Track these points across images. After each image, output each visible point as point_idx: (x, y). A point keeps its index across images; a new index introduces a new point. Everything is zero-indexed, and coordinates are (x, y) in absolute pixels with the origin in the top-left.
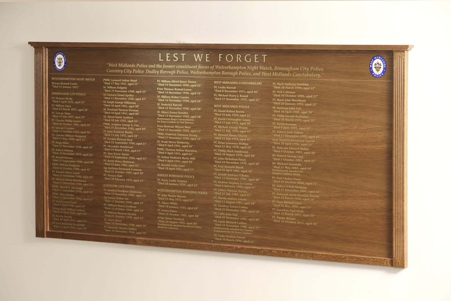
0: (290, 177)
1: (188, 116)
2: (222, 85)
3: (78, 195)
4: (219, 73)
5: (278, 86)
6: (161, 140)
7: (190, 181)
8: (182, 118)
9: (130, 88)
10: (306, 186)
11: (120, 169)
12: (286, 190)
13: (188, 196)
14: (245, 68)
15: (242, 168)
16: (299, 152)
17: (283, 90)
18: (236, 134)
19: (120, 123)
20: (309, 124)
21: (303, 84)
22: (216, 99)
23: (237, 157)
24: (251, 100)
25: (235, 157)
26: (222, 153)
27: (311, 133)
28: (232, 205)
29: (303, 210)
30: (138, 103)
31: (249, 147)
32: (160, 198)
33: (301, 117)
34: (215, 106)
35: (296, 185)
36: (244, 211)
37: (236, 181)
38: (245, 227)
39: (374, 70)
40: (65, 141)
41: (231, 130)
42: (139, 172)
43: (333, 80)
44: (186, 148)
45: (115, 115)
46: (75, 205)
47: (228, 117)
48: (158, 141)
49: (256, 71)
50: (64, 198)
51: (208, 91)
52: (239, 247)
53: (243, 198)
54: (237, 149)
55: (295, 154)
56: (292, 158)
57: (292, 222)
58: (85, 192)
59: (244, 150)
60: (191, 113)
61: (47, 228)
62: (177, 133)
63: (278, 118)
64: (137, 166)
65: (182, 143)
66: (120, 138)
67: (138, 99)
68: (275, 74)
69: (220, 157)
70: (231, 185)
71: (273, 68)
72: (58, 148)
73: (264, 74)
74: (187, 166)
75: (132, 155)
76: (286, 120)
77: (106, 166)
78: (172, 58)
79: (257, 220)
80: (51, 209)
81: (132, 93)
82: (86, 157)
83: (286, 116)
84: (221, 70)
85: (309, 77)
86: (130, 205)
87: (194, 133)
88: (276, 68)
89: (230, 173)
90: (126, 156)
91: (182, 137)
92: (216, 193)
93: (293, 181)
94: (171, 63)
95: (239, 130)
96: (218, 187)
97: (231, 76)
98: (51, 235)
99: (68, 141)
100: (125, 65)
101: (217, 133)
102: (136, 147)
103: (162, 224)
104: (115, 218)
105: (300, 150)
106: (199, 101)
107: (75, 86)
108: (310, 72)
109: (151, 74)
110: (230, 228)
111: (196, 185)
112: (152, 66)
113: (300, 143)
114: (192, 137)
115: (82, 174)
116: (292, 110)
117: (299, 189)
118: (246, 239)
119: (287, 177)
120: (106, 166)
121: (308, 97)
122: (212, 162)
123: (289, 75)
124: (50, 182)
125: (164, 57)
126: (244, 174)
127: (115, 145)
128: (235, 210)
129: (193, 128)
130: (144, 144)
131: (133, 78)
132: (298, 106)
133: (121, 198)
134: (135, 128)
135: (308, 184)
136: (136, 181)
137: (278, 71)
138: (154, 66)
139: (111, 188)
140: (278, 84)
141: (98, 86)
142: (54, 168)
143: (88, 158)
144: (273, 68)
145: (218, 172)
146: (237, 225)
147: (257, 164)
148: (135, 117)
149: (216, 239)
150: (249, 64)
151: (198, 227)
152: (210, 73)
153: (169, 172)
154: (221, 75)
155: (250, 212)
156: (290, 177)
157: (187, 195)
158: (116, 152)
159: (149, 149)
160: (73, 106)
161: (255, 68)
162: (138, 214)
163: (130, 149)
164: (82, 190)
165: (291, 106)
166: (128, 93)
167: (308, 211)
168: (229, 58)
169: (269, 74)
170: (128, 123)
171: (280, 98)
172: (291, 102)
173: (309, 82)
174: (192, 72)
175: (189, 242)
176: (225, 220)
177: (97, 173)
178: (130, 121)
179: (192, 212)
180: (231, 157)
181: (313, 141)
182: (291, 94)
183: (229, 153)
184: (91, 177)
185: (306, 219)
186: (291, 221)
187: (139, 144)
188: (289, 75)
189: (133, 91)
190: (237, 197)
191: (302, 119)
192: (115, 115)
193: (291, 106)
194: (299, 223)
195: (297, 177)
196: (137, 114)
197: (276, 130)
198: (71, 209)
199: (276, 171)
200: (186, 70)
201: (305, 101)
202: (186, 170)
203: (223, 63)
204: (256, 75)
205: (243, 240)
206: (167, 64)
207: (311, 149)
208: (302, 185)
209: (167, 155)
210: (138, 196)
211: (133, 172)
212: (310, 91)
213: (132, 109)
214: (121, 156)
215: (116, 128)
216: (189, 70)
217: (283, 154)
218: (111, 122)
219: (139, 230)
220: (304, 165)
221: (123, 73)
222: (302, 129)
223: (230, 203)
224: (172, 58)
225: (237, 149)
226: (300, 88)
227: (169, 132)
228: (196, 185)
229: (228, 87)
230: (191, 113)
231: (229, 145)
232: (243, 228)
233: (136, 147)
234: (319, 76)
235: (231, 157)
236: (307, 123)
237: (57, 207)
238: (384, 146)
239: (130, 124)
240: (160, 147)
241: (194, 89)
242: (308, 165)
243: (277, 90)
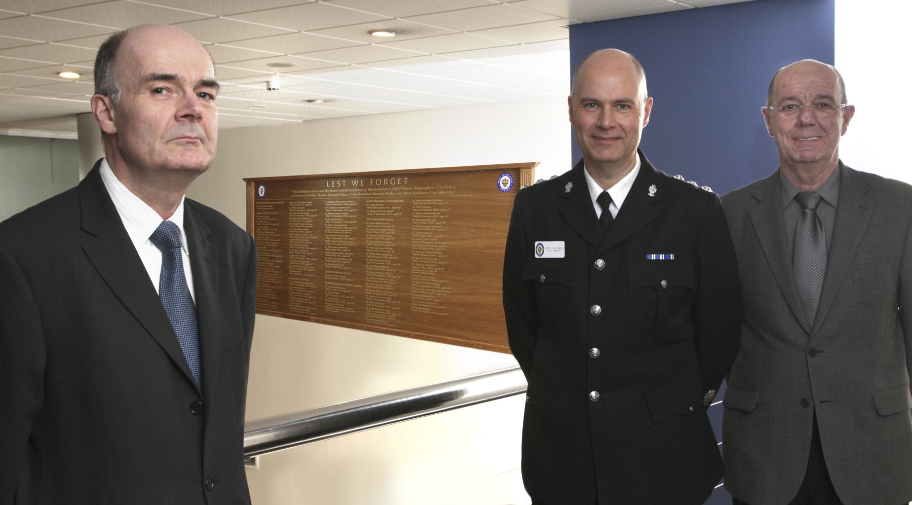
3: (272, 284)
7: (348, 277)
9: (307, 208)
13: (347, 288)
27: (444, 240)
30: (312, 218)
39: (502, 185)
42: (313, 269)
43: (464, 196)
51: (362, 209)
60: (349, 225)
74: (346, 265)
75: (308, 256)
84: (372, 192)
94: (336, 188)
100: (304, 191)
102: (311, 251)
103: (328, 308)
107: (271, 208)
108: (444, 190)
122: (365, 262)
123: (426, 193)
125: (330, 184)
129: (351, 236)
141: (286, 207)
153: (333, 270)
159: (319, 253)
160: (270, 222)
162: (312, 300)
167: (440, 304)
168: (379, 182)
179: (349, 300)
185: (439, 310)
186: (426, 311)
188: (426, 193)
199: (414, 270)
203: (374, 186)
204: (399, 194)
206: (333, 189)
207: (444, 253)
216: (348, 193)
219: (312, 311)
230: (349, 225)
233: (311, 251)
241: (352, 207)
242: (441, 266)
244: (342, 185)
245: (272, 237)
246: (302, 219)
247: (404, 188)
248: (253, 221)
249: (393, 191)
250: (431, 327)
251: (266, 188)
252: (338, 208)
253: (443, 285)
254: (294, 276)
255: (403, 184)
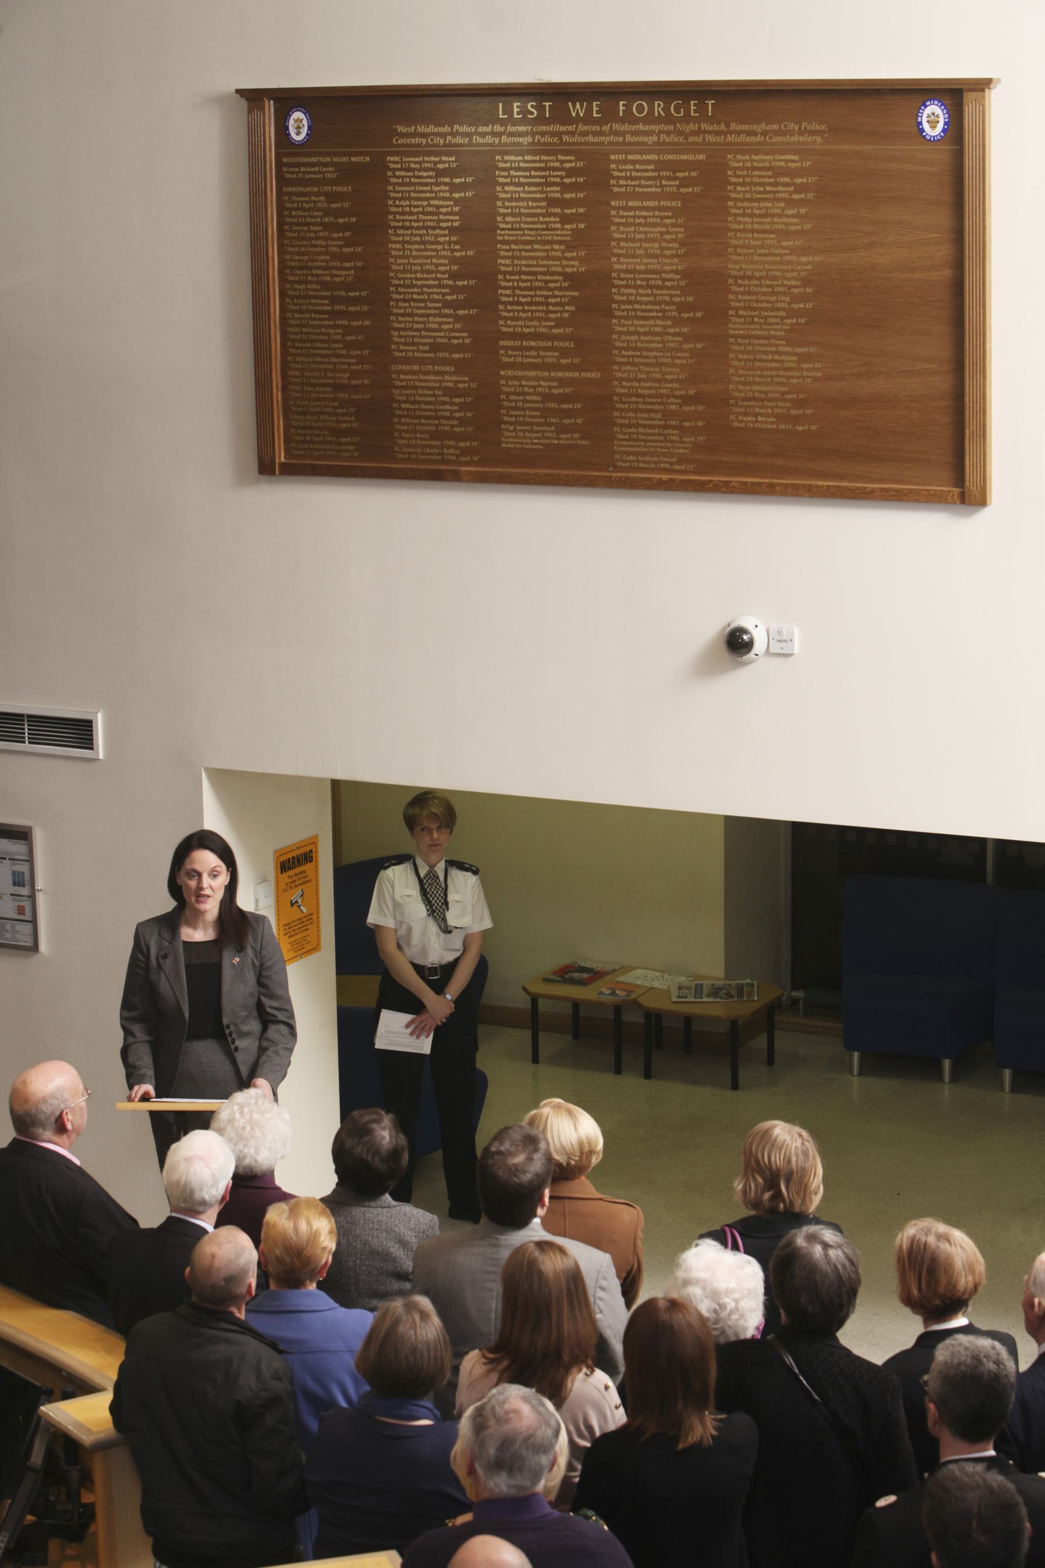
7: (565, 353)
9: (440, 173)
13: (562, 382)
27: (805, 251)
30: (457, 202)
39: (926, 126)
42: (463, 338)
43: (847, 147)
74: (560, 323)
75: (447, 305)
84: (623, 134)
100: (431, 129)
102: (455, 290)
107: (330, 173)
108: (801, 133)
122: (609, 314)
123: (759, 139)
125: (508, 111)
129: (569, 247)
141: (378, 172)
153: (523, 336)
159: (479, 286)
160: (327, 212)
167: (799, 403)
168: (640, 109)
179: (569, 413)
185: (796, 420)
188: (759, 139)
199: (736, 327)
203: (629, 118)
207: (806, 282)
216: (559, 135)
230: (565, 219)
233: (455, 290)
241: (570, 173)
242: (798, 314)
245: (335, 257)
247: (704, 126)
248: (273, 211)
249: (680, 133)
250: (779, 462)
255: (703, 117)
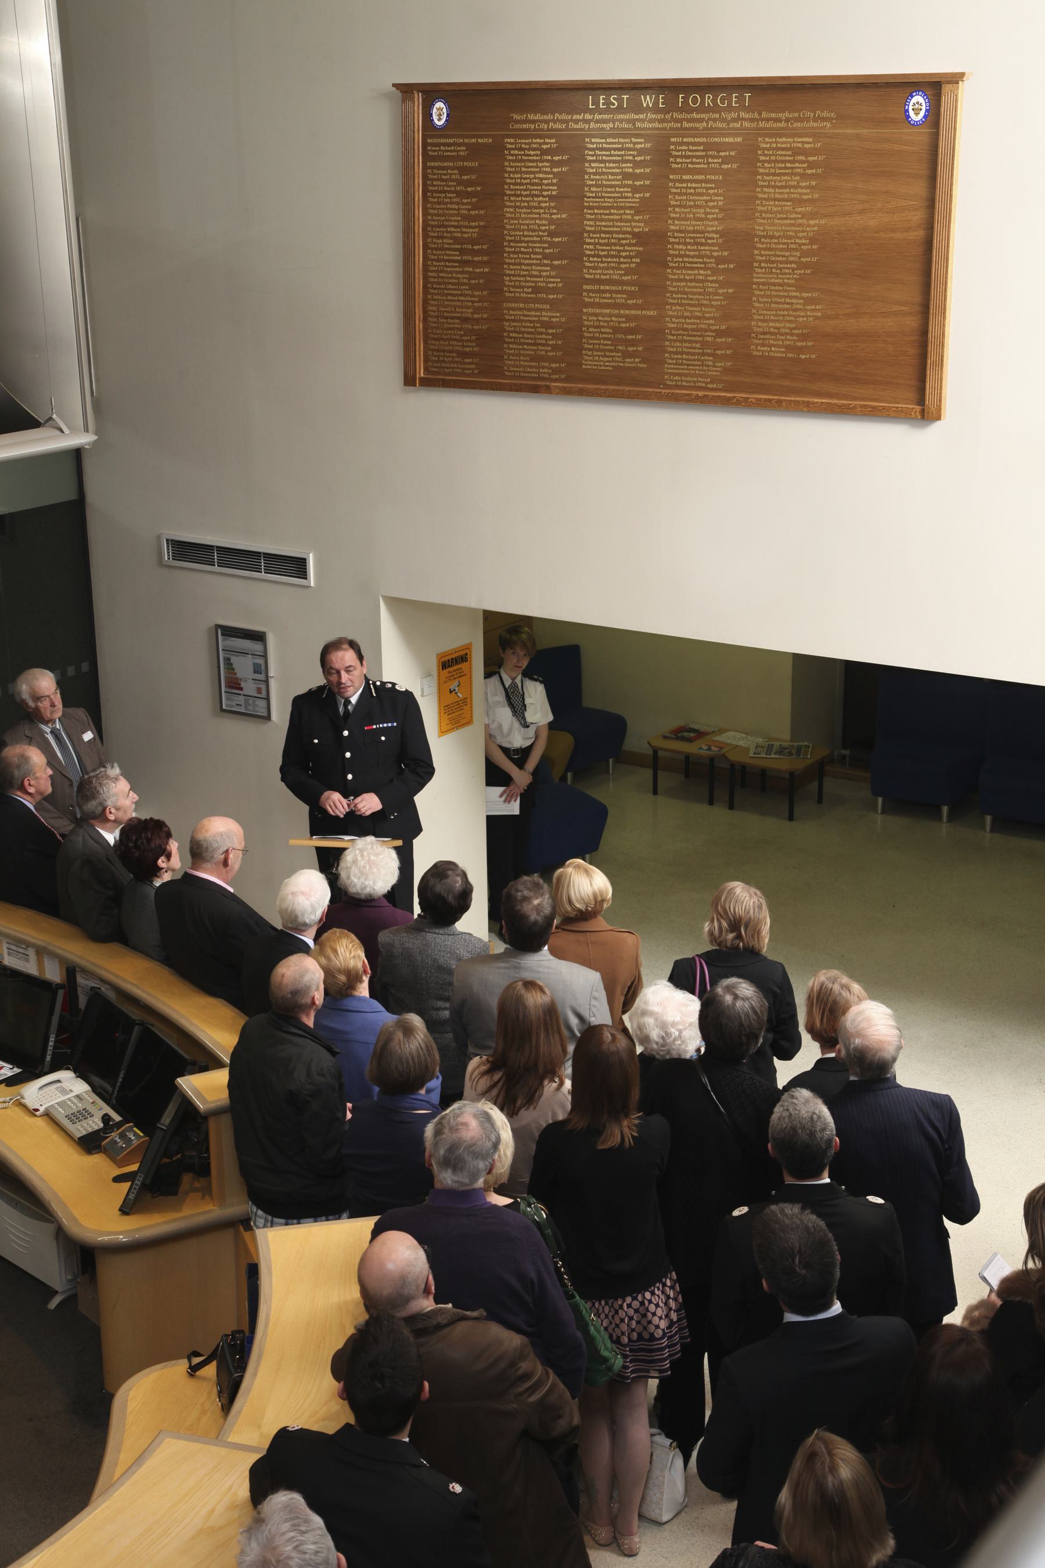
0: (779, 285)
1: (630, 195)
2: (682, 144)
4: (679, 125)
5: (767, 143)
6: (589, 232)
7: (631, 295)
8: (622, 197)
9: (544, 152)
10: (802, 298)
11: (528, 279)
12: (773, 305)
13: (628, 319)
14: (717, 116)
15: (709, 272)
16: (793, 246)
17: (773, 149)
18: (702, 219)
19: (528, 207)
20: (811, 201)
21: (804, 140)
22: (674, 166)
23: (702, 257)
24: (725, 167)
25: (698, 257)
26: (680, 250)
27: (812, 216)
28: (693, 330)
29: (797, 335)
30: (556, 175)
31: (720, 241)
32: (586, 323)
33: (800, 190)
34: (671, 177)
35: (788, 297)
36: (710, 339)
37: (700, 294)
38: (711, 363)
40: (446, 238)
41: (694, 214)
42: (556, 283)
43: (850, 131)
44: (626, 244)
45: (521, 195)
46: (461, 336)
47: (691, 194)
48: (585, 235)
49: (734, 120)
50: (446, 326)
51: (661, 156)
52: (701, 394)
53: (709, 318)
54: (702, 244)
55: (788, 249)
56: (783, 256)
57: (779, 355)
58: (476, 316)
59: (713, 245)
60: (635, 190)
61: (421, 373)
62: (613, 220)
63: (765, 193)
64: (553, 273)
65: (620, 236)
66: (528, 230)
67: (555, 170)
68: (761, 125)
69: (676, 256)
70: (692, 299)
71: (760, 114)
72: (436, 249)
73: (746, 124)
75: (546, 257)
76: (777, 196)
77: (507, 275)
78: (608, 103)
79: (728, 352)
80: (425, 342)
81: (547, 161)
82: (479, 262)
83: (777, 190)
84: (680, 121)
85: (813, 128)
86: (542, 333)
87: (639, 221)
88: (764, 115)
89: (691, 281)
90: (537, 259)
91: (621, 227)
92: (670, 313)
93: (784, 291)
94: (607, 111)
95: (706, 213)
96: (672, 304)
97: (697, 129)
98: (428, 383)
99: (451, 238)
101: (674, 219)
102: (552, 245)
103: (589, 362)
104: (519, 355)
105: (795, 243)
106: (648, 170)
107: (463, 151)
108: (815, 120)
109: (576, 130)
110: (688, 365)
111: (639, 302)
112: (578, 117)
113: (795, 232)
114: (636, 227)
115: (473, 288)
116: (786, 181)
117: (792, 304)
118: (712, 382)
119: (775, 285)
120: (507, 275)
121: (811, 159)
123: (783, 125)
124: (425, 301)
125: (596, 102)
126: (712, 282)
127: (521, 242)
128: (697, 339)
129: (638, 212)
130: (565, 239)
131: (550, 137)
132: (796, 174)
133: (528, 324)
134: (551, 214)
135: (805, 295)
136: (551, 297)
137: (768, 120)
138: (581, 117)
139: (514, 309)
140: (767, 139)
141: (497, 150)
142: (431, 280)
143: (481, 264)
144: (760, 114)
145: (673, 280)
146: (698, 360)
147: (731, 266)
148: (551, 197)
149: (668, 383)
150: (724, 109)
151: (642, 365)
152: (665, 125)
153: (600, 282)
154: (681, 129)
155: (719, 340)
156: (779, 285)
157: (626, 316)
158: (523, 253)
159: (571, 246)
160: (460, 183)
161: (734, 115)
162: (554, 348)
163: (544, 248)
164: (472, 314)
165: (784, 174)
166: (542, 161)
167: (803, 337)
168: (695, 100)
169: (754, 125)
170: (541, 208)
171: (769, 162)
172: (786, 168)
173: (813, 135)
174: (638, 125)
175: (627, 388)
176: (682, 353)
177: (494, 287)
178: (544, 205)
179: (633, 343)
180: (693, 257)
181: (816, 229)
182: (785, 155)
183: (690, 250)
184: (485, 293)
186: (777, 353)
187: (556, 240)
188: (783, 125)
189: (549, 158)
190: (699, 318)
191: (801, 194)
192: (521, 195)
193: (784, 174)
194: (789, 355)
195: (789, 285)
196: (554, 193)
197: (761, 212)
198: (455, 343)
199: (759, 276)
200: (628, 121)
201: (805, 165)
202: (625, 278)
203: (686, 109)
204: (733, 125)
205: (707, 383)
206: (601, 112)
207: (812, 241)
208: (796, 297)
209: (599, 256)
210: (554, 320)
211: (547, 283)
212: (814, 149)
213: (547, 185)
214: (530, 259)
215: (523, 216)
216: (633, 121)
217: (770, 249)
218: (516, 207)
219: (555, 371)
220: (801, 266)
221: (535, 130)
222: (800, 209)
223: (690, 327)
224: (608, 103)
225: (702, 244)
226: (800, 145)
227: (601, 220)
228: (639, 302)
229: (691, 147)
230: (635, 190)
231: (690, 238)
232: (707, 366)
233: (552, 245)
234: (828, 125)
235: (693, 257)
236: (808, 200)
237: (435, 339)
238: (921, 233)
239: (544, 208)
240: (589, 244)
241: (641, 152)
242: (805, 266)
243: (764, 149)
244: (620, 105)
246: (533, 174)
247: (743, 114)
248: (419, 181)
250: (786, 383)
251: (450, 107)
252: (612, 150)
253: (809, 301)
254: (516, 300)
255: (742, 107)
